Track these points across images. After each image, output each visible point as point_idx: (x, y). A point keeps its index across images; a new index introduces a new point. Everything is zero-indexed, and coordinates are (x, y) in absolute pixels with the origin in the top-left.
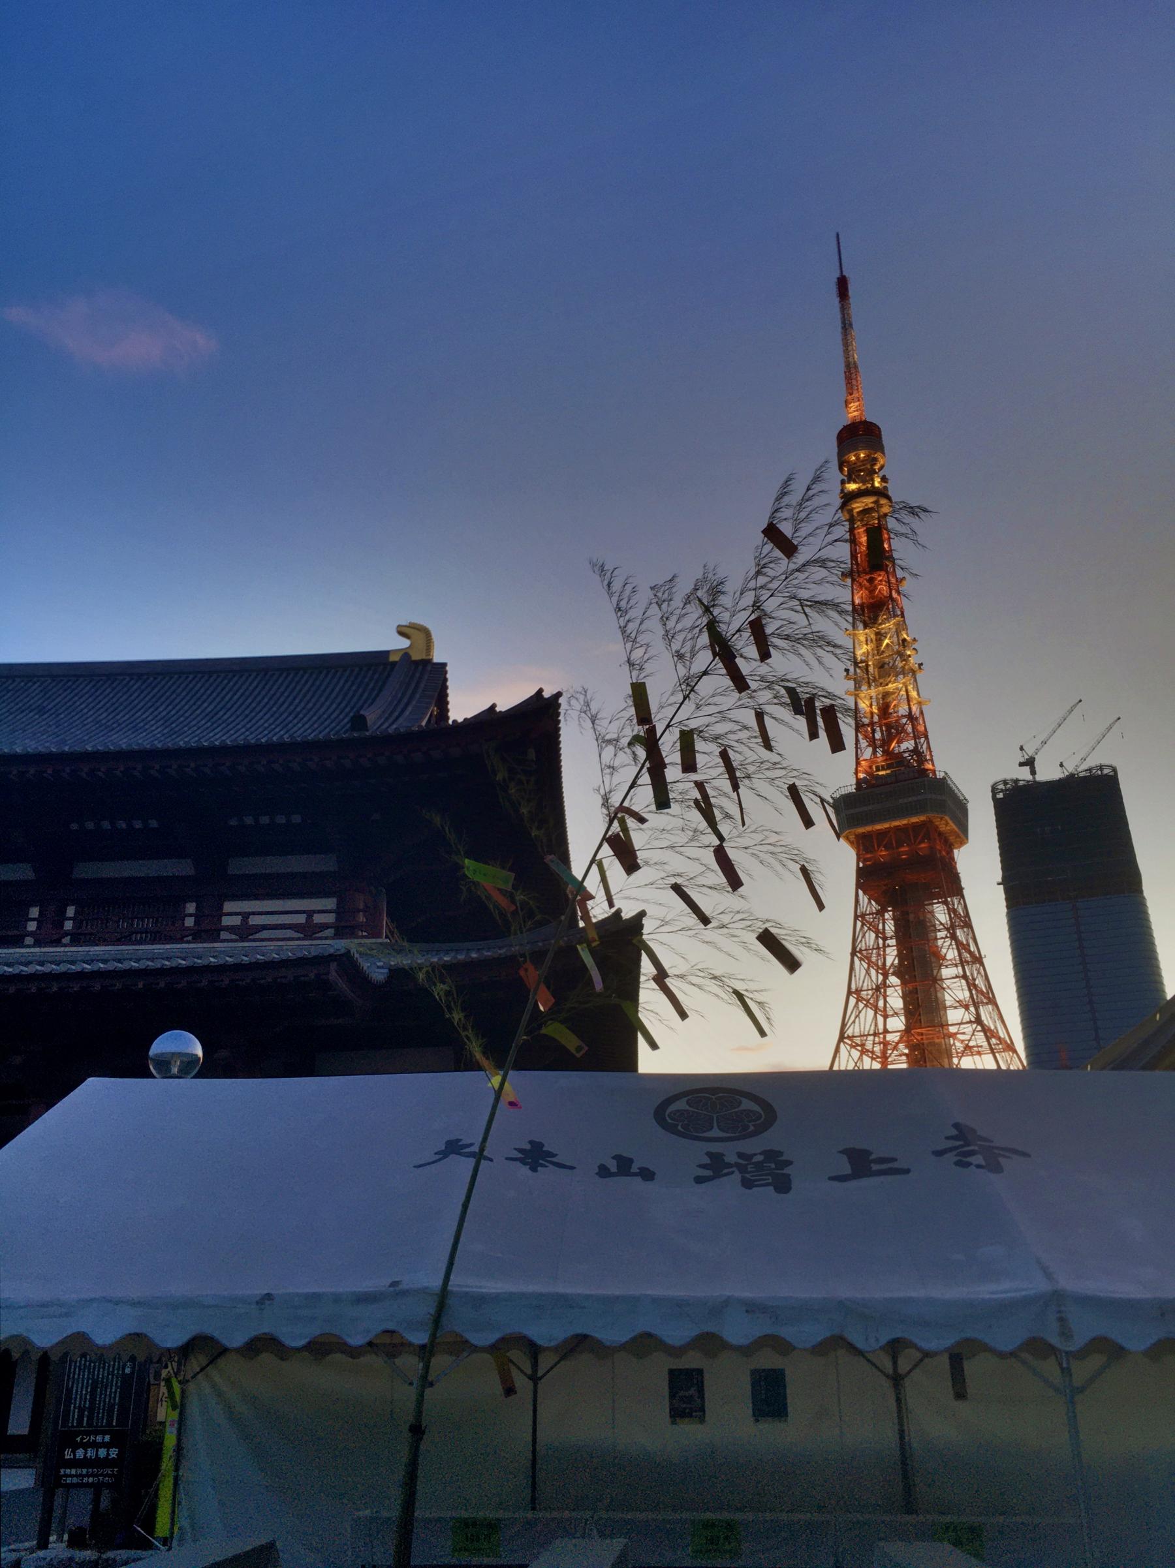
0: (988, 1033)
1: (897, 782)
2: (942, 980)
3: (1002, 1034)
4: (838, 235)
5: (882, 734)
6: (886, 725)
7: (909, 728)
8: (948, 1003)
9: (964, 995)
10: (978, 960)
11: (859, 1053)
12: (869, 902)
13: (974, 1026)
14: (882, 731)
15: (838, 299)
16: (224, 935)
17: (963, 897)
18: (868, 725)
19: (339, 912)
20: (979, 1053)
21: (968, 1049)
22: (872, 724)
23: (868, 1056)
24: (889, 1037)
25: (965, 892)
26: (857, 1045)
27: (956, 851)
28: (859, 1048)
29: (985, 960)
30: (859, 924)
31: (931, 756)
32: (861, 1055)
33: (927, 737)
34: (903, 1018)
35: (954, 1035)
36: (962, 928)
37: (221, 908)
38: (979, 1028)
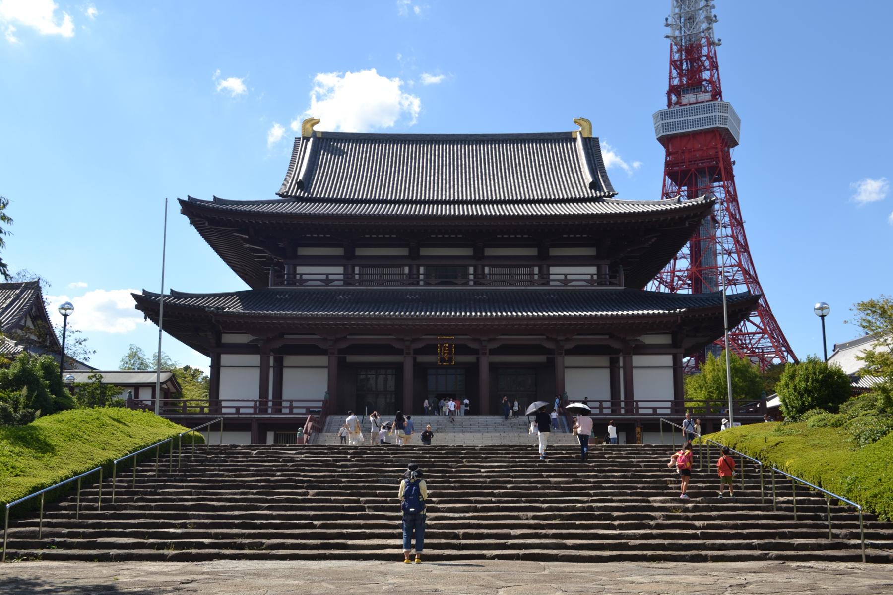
2: (717, 238)
3: (752, 273)
5: (687, 66)
7: (707, 64)
8: (718, 252)
9: (730, 245)
10: (740, 223)
11: (658, 283)
12: (672, 183)
13: (735, 269)
14: (687, 64)
16: (551, 283)
17: (733, 181)
18: (677, 61)
19: (599, 274)
20: (735, 284)
21: (731, 282)
22: (681, 60)
23: (663, 284)
24: (677, 273)
25: (735, 178)
26: (659, 278)
27: (731, 150)
28: (659, 280)
29: (744, 224)
31: (720, 83)
32: (659, 284)
33: (717, 70)
34: (689, 260)
35: (721, 273)
36: (732, 202)
37: (548, 270)
38: (740, 269)
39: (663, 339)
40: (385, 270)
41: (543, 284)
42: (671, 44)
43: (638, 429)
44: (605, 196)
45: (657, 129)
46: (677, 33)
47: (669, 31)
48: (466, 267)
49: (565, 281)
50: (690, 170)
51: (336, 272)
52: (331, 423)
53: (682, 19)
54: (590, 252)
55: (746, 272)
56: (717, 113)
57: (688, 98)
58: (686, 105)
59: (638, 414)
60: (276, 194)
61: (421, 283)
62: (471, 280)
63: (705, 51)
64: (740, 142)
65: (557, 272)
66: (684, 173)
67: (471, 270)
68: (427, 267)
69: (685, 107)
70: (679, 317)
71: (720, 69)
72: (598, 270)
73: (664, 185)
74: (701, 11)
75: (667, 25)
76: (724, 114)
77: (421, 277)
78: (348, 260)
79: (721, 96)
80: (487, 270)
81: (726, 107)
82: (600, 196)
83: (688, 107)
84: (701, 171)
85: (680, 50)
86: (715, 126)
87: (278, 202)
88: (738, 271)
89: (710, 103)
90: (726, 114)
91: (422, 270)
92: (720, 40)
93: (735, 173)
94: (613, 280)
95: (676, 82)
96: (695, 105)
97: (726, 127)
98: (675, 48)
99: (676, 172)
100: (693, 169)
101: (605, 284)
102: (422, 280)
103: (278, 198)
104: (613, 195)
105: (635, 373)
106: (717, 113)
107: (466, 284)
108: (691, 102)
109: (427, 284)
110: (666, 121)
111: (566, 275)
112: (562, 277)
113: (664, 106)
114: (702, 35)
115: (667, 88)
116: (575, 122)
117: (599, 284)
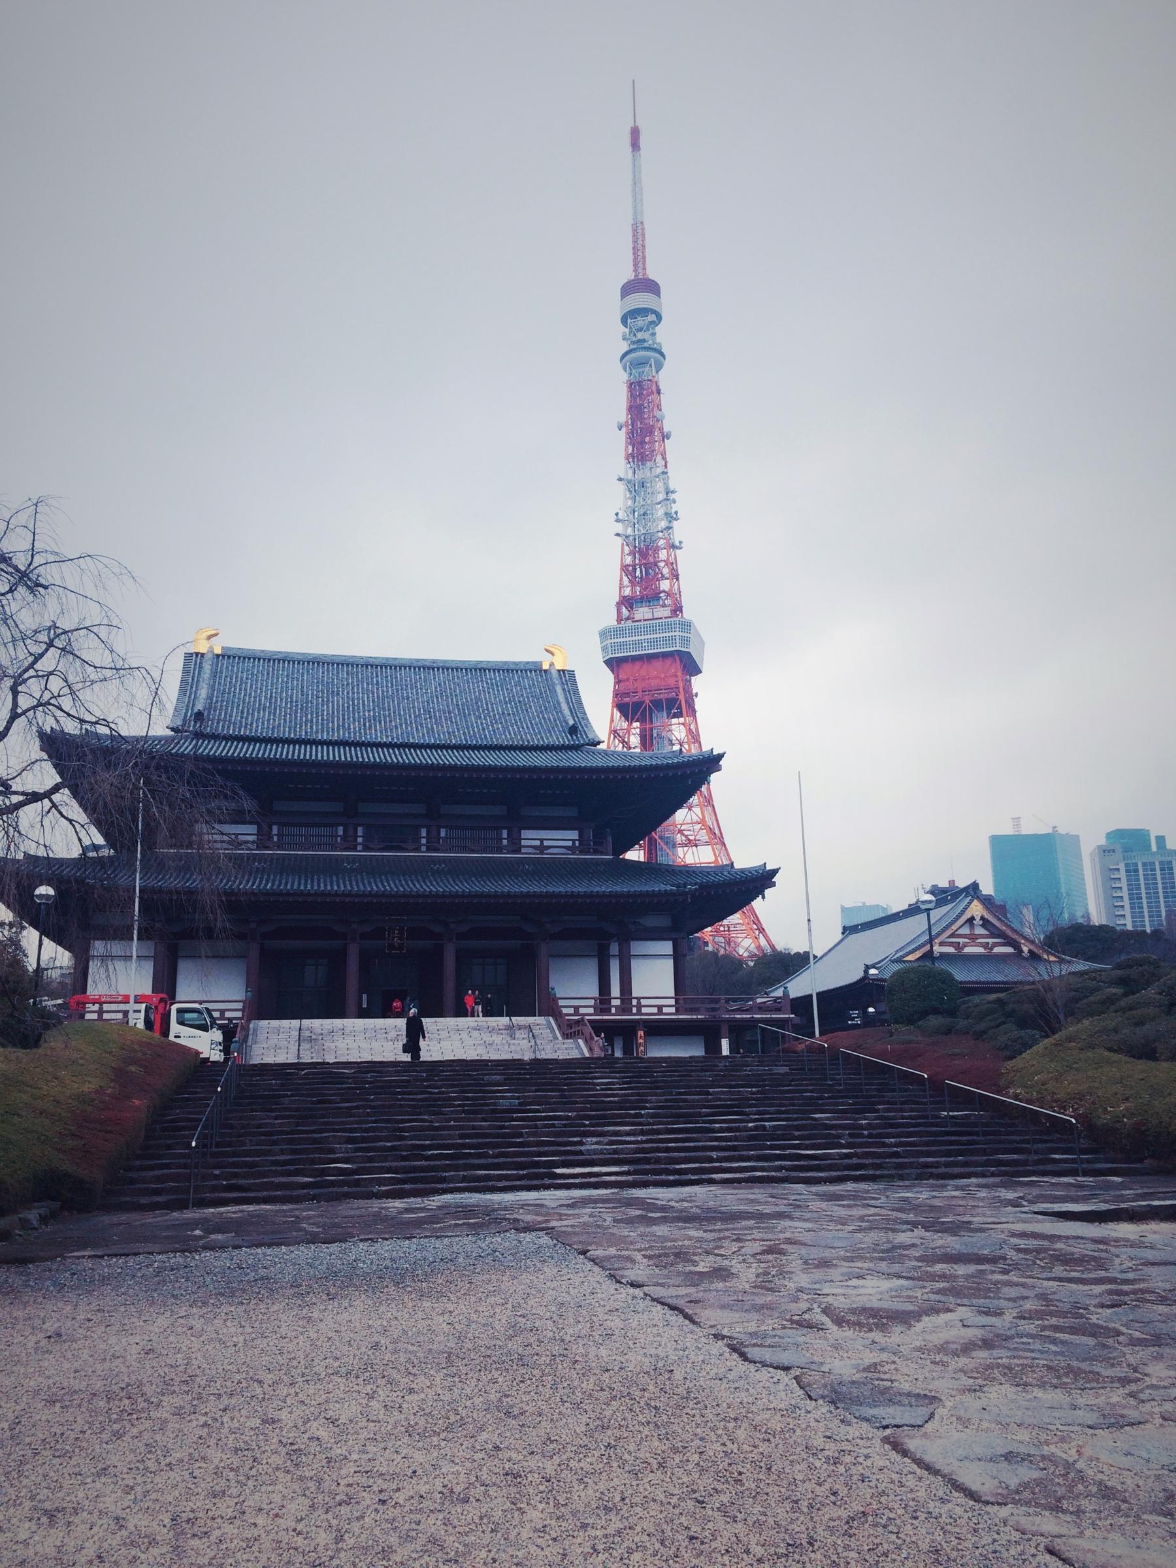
0: (711, 831)
3: (717, 832)
5: (641, 572)
6: (645, 564)
7: (666, 571)
15: (630, 149)
16: (523, 850)
17: (695, 717)
20: (696, 846)
21: (692, 843)
25: (697, 714)
30: (612, 736)
35: (680, 831)
39: (662, 921)
40: (313, 831)
41: (514, 852)
42: (623, 544)
43: (641, 1033)
44: (588, 745)
45: (604, 649)
46: (629, 531)
47: (619, 528)
48: (417, 828)
49: (542, 848)
50: (644, 702)
51: (247, 833)
52: (255, 1030)
53: (636, 514)
54: (572, 812)
55: (711, 831)
56: (677, 633)
57: (642, 612)
59: (639, 1013)
60: (167, 727)
61: (360, 847)
62: (424, 845)
63: (663, 555)
64: (705, 668)
65: (531, 837)
66: (638, 705)
67: (424, 833)
68: (367, 827)
69: (639, 623)
70: (689, 896)
71: (680, 578)
72: (581, 835)
73: (612, 721)
74: (659, 506)
75: (618, 521)
76: (686, 635)
77: (360, 840)
78: (264, 817)
79: (681, 611)
80: (443, 833)
81: (687, 626)
82: (583, 745)
83: (642, 623)
84: (657, 705)
85: (633, 553)
87: (173, 738)
88: (701, 829)
89: (669, 620)
90: (688, 635)
91: (360, 831)
92: (680, 542)
93: (697, 707)
94: (599, 848)
95: (627, 592)
96: (651, 622)
97: (687, 650)
98: (627, 549)
99: (627, 704)
100: (647, 702)
101: (588, 853)
102: (360, 844)
103: (170, 733)
104: (599, 743)
105: (634, 964)
106: (677, 633)
107: (417, 849)
109: (366, 848)
111: (542, 840)
112: (538, 843)
113: (613, 622)
114: (660, 535)
115: (617, 599)
116: (547, 650)
117: (581, 852)
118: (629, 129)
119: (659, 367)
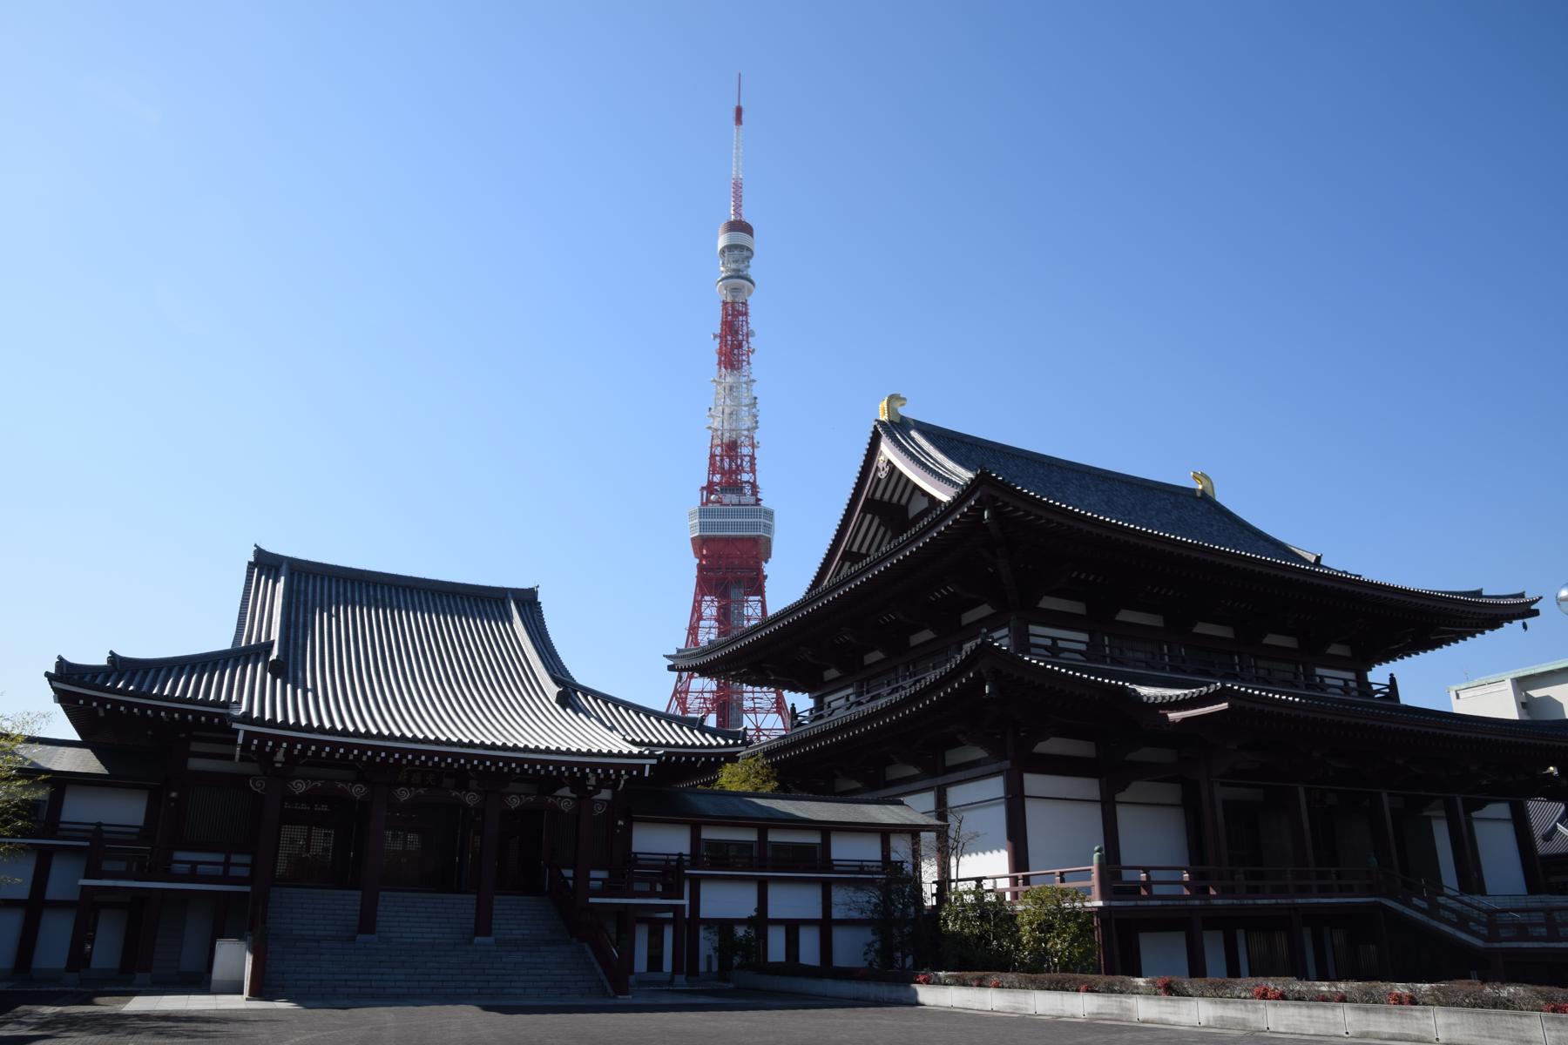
1: (739, 505)
4: (740, 75)
56: (762, 520)
58: (728, 505)
76: (769, 522)
86: (758, 533)
108: (733, 503)
110: (755, 520)
118: (734, 107)
119: (750, 292)
